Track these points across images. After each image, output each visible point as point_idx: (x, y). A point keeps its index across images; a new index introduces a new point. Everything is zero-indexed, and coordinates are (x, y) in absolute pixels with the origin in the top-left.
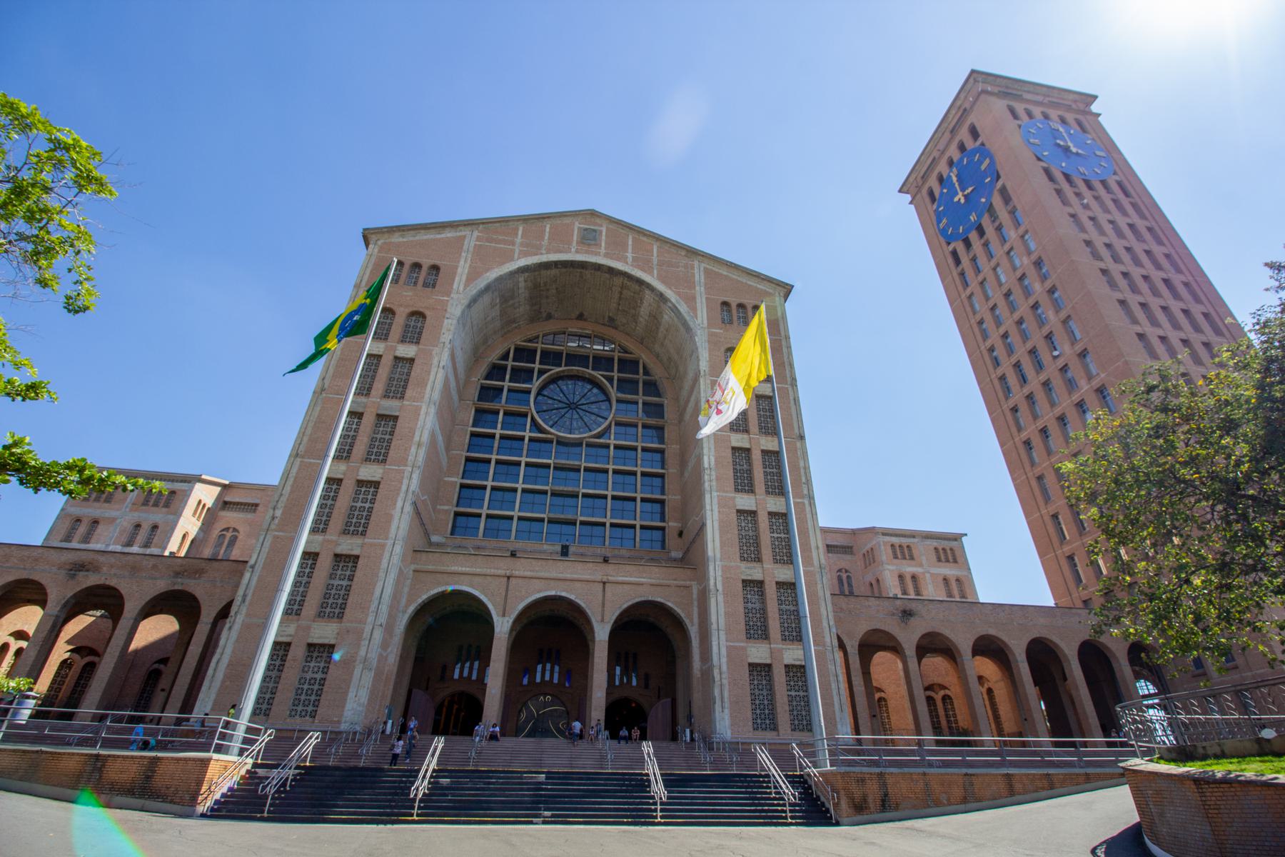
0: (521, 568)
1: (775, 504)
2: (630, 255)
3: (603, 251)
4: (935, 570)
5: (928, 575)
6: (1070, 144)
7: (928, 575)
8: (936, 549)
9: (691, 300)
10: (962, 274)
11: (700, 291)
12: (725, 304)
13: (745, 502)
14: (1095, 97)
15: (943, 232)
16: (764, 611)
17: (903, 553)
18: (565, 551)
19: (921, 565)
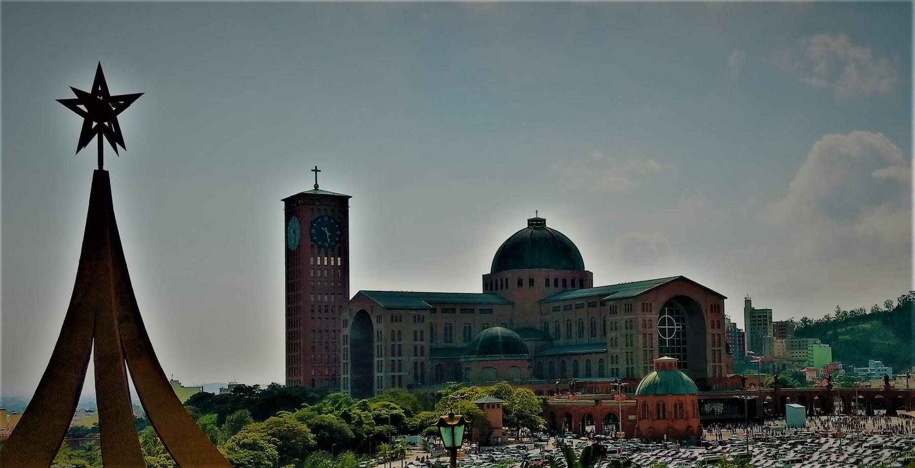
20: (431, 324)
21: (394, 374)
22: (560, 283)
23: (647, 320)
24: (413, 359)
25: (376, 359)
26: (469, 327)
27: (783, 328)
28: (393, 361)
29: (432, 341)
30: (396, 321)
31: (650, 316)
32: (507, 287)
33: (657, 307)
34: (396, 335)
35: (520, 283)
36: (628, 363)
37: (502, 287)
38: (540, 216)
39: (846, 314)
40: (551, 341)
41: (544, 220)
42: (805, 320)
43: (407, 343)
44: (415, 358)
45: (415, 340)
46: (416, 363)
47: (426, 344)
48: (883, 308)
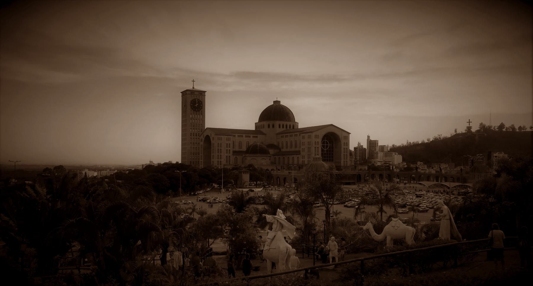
20: (233, 141)
21: (218, 160)
22: (285, 127)
23: (317, 142)
24: (226, 154)
25: (212, 154)
27: (382, 147)
28: (218, 155)
29: (233, 148)
30: (220, 140)
31: (318, 140)
32: (264, 128)
33: (321, 137)
36: (308, 159)
37: (262, 128)
38: (278, 100)
39: (410, 144)
40: (280, 149)
41: (280, 102)
42: (393, 145)
46: (227, 156)
48: (426, 141)
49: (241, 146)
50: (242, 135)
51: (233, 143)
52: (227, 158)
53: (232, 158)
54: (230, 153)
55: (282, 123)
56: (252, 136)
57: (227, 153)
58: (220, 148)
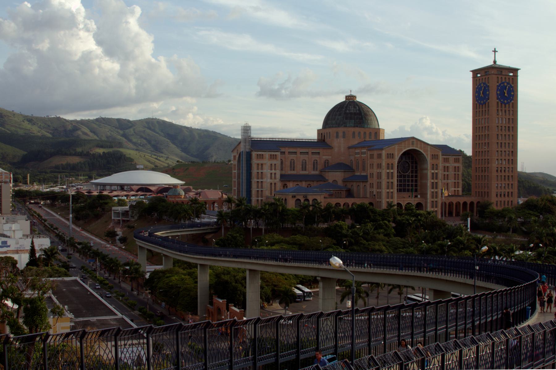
0: (405, 199)
1: (436, 190)
2: (419, 146)
3: (415, 146)
4: (453, 165)
5: (451, 166)
6: (506, 93)
7: (451, 166)
8: (455, 159)
9: (427, 155)
10: (477, 112)
11: (429, 152)
12: (433, 155)
13: (433, 190)
14: (520, 69)
15: (476, 96)
16: (433, 205)
17: (446, 160)
18: (409, 196)
19: (450, 164)
20: (281, 160)
21: (258, 189)
24: (269, 180)
26: (305, 162)
28: (258, 182)
29: (282, 169)
34: (260, 167)
35: (337, 137)
38: (353, 94)
41: (355, 97)
43: (267, 171)
44: (271, 180)
45: (271, 169)
46: (271, 184)
47: (278, 173)
49: (294, 167)
50: (296, 151)
51: (282, 163)
52: (271, 187)
53: (279, 186)
54: (275, 178)
55: (357, 130)
56: (310, 151)
57: (271, 178)
58: (260, 171)
